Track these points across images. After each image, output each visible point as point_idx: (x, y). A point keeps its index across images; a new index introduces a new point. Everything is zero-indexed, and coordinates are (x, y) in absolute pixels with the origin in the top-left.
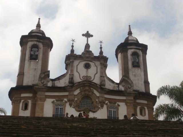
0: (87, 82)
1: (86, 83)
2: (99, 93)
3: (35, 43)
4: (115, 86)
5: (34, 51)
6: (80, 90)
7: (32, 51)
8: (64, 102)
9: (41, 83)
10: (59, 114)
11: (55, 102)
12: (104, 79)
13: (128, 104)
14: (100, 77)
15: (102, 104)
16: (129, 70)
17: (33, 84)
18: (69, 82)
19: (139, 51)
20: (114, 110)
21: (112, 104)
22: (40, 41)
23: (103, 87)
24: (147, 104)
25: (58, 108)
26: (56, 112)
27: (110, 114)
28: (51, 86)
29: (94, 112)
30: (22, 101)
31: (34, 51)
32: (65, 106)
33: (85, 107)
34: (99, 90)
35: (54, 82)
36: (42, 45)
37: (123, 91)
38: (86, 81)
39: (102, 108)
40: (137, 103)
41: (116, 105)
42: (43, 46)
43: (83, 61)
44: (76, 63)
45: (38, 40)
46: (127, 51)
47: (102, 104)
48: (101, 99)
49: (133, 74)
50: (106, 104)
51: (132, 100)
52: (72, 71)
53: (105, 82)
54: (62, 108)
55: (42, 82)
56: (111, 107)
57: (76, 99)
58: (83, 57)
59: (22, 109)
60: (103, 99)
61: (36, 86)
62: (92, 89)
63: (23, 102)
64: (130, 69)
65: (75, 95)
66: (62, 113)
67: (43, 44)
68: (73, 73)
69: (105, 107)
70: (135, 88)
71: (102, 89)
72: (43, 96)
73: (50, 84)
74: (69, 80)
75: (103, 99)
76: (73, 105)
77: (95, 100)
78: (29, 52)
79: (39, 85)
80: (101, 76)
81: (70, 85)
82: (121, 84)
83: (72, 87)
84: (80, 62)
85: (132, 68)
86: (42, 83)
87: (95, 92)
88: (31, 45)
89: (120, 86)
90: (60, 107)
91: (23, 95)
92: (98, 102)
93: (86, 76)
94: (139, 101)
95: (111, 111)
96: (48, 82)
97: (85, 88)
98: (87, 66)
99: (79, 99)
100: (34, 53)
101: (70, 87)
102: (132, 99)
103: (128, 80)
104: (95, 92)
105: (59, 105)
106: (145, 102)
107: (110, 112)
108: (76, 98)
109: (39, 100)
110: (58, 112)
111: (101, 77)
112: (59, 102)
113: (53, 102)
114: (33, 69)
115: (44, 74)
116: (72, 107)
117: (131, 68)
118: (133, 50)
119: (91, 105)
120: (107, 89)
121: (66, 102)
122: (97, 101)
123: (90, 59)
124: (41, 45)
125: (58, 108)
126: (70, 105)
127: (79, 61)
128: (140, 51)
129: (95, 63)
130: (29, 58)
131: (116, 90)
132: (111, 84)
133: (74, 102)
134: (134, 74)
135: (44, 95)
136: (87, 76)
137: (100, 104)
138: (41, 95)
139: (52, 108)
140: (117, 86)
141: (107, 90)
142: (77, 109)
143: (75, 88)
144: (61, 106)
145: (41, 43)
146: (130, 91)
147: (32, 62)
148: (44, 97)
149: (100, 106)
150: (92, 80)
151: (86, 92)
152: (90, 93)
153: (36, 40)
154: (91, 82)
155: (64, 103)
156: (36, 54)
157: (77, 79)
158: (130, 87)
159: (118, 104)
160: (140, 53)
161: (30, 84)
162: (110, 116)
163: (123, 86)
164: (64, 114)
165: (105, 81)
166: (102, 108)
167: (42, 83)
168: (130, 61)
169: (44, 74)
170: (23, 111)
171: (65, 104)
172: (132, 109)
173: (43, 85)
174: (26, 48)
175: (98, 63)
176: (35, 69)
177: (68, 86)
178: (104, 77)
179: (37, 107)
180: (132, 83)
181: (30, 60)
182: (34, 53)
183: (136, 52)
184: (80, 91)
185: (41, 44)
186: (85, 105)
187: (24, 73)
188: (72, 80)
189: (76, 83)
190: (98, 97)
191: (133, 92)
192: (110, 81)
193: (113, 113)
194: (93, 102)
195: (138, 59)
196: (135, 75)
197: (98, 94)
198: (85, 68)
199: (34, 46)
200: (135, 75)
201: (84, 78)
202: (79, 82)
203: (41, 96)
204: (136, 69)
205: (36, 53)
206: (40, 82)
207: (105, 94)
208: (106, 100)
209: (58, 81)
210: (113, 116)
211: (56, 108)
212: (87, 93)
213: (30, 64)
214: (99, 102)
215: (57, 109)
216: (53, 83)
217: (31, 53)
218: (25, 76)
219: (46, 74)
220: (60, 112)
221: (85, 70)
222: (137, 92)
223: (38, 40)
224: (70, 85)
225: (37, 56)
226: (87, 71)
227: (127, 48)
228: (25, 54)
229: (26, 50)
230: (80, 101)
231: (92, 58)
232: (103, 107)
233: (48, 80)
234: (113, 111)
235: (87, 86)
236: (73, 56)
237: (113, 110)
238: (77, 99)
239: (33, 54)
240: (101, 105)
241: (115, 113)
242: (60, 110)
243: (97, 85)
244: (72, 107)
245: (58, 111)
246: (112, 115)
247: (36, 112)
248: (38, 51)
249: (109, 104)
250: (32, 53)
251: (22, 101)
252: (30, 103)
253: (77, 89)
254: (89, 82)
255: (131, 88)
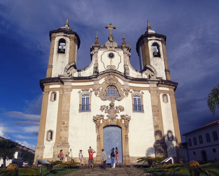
0: (112, 71)
1: (110, 72)
2: (124, 81)
3: (62, 37)
4: (138, 74)
5: (62, 46)
6: (105, 79)
7: (60, 45)
8: (89, 91)
9: (66, 74)
10: (85, 104)
11: (81, 92)
12: (128, 68)
13: (152, 92)
14: (124, 66)
15: (127, 92)
16: (150, 60)
17: (58, 75)
18: (94, 72)
19: (159, 42)
20: (139, 98)
21: (137, 92)
22: (67, 36)
23: (127, 75)
24: (169, 91)
25: (84, 98)
26: (82, 102)
27: (135, 102)
28: (77, 76)
29: (119, 100)
30: (51, 92)
31: (62, 46)
32: (91, 96)
33: (110, 95)
34: (124, 79)
35: (80, 72)
36: (69, 40)
37: (146, 79)
38: (111, 70)
39: (127, 97)
40: (160, 90)
41: (141, 92)
42: (70, 40)
43: (107, 51)
44: (100, 52)
45: (65, 35)
46: (148, 42)
47: (127, 91)
48: (125, 87)
49: (154, 64)
50: (131, 92)
51: (156, 88)
52: (97, 61)
53: (129, 71)
54: (88, 98)
55: (68, 73)
56: (135, 95)
57: (101, 88)
58: (106, 47)
59: (51, 100)
60: (128, 87)
61: (62, 77)
62: (116, 77)
63: (52, 94)
64: (151, 59)
65: (99, 84)
66: (88, 103)
67: (70, 39)
68: (98, 63)
69: (130, 94)
70: (158, 76)
71: (126, 77)
72: (70, 86)
73: (76, 75)
74: (94, 69)
75: (128, 87)
76: (99, 95)
77: (119, 88)
78: (57, 46)
79: (64, 76)
80: (125, 65)
81: (95, 74)
82: (144, 72)
83: (96, 77)
84: (104, 52)
85: (153, 58)
86: (68, 74)
87: (120, 80)
88: (59, 40)
89: (143, 74)
90: (86, 97)
91: (51, 87)
92: (123, 90)
93: (110, 65)
94: (160, 88)
95: (136, 99)
96: (74, 72)
97: (110, 77)
98: (111, 56)
99: (104, 88)
100: (62, 48)
101: (95, 76)
102: (155, 86)
103: (151, 68)
104: (120, 80)
105: (86, 95)
106: (167, 89)
107: (134, 100)
108: (101, 87)
109: (65, 90)
110: (84, 102)
111: (125, 66)
112: (85, 92)
113: (79, 92)
114: (61, 62)
115: (70, 65)
116: (97, 96)
117: (152, 58)
118: (153, 41)
119: (116, 94)
120: (131, 77)
121: (91, 92)
122: (122, 90)
123: (113, 49)
124: (67, 40)
125: (84, 98)
126: (96, 94)
127: (103, 51)
128: (160, 42)
129: (118, 53)
130: (56, 51)
131: (139, 78)
132: (135, 72)
133: (99, 91)
134: (155, 63)
135: (71, 86)
136: (111, 65)
137: (124, 92)
138: (67, 86)
139: (79, 97)
140: (141, 74)
141: (131, 78)
142: (103, 97)
143: (100, 78)
144: (87, 96)
145: (68, 37)
146: (155, 79)
147: (59, 55)
148: (71, 87)
149: (125, 95)
150: (117, 69)
151: (111, 81)
152: (115, 82)
153: (64, 34)
154: (116, 70)
155: (89, 92)
156: (63, 48)
157: (101, 69)
158: (153, 75)
159: (142, 92)
160: (160, 43)
161: (57, 76)
162: (135, 104)
163: (146, 74)
164: (90, 104)
165: (129, 69)
166: (127, 97)
167: (68, 74)
168: (151, 51)
169: (70, 65)
170: (52, 102)
171: (91, 94)
172: (156, 96)
173: (69, 76)
174: (54, 43)
175: (121, 52)
176: (63, 62)
177: (93, 75)
178: (128, 65)
179: (64, 97)
180: (155, 71)
181: (58, 54)
182: (62, 48)
183: (156, 43)
184: (105, 80)
185: (68, 38)
186: (110, 94)
187: (52, 66)
188: (96, 69)
189: (100, 73)
190: (123, 85)
191: (157, 80)
192: (134, 70)
193: (138, 101)
194: (118, 91)
195: (158, 49)
196: (156, 64)
197: (122, 83)
198: (110, 58)
199: (62, 41)
200: (156, 64)
201: (109, 67)
202: (104, 72)
203: (68, 87)
204: (157, 58)
205: (64, 48)
206: (66, 73)
207: (130, 82)
208: (130, 89)
209: (84, 71)
210: (137, 104)
211: (83, 98)
212: (112, 82)
213: (58, 58)
214: (124, 90)
215: (83, 99)
216: (79, 74)
217: (58, 48)
218: (53, 69)
219: (71, 65)
220: (86, 102)
221: (109, 59)
222: (160, 80)
223: (65, 35)
224: (95, 74)
225: (64, 50)
226: (111, 62)
227: (148, 39)
228: (54, 48)
229: (54, 45)
230: (105, 91)
231: (116, 47)
232: (128, 95)
233: (74, 71)
234: (138, 99)
235: (111, 74)
236: (97, 46)
237: (137, 98)
238: (102, 88)
239: (61, 48)
240: (126, 93)
241: (140, 101)
242: (86, 100)
243: (122, 74)
244: (98, 96)
245: (84, 100)
246: (136, 102)
247: (63, 102)
248: (65, 45)
249: (133, 92)
250: (60, 47)
251: (51, 92)
252: (58, 93)
253: (102, 78)
254: (114, 71)
255: (155, 75)
